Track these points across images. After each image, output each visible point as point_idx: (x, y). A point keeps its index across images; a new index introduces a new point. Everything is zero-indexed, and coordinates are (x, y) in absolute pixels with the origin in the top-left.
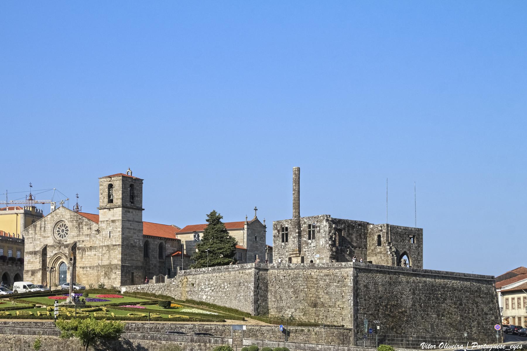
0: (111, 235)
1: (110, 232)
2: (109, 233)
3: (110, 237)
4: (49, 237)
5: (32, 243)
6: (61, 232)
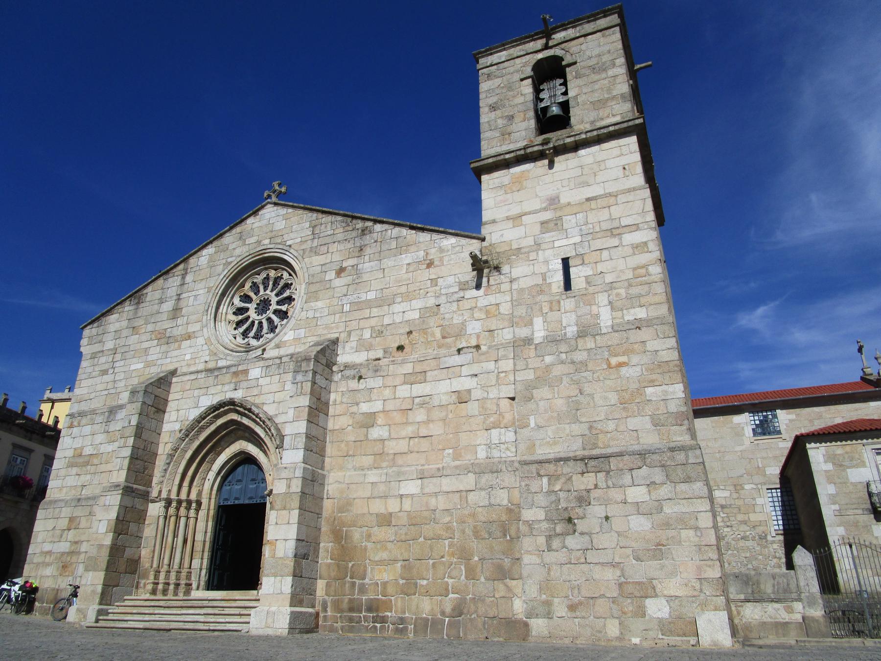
0: (572, 276)
1: (566, 262)
2: (560, 266)
3: (568, 285)
4: (189, 338)
5: (111, 371)
6: (252, 306)
